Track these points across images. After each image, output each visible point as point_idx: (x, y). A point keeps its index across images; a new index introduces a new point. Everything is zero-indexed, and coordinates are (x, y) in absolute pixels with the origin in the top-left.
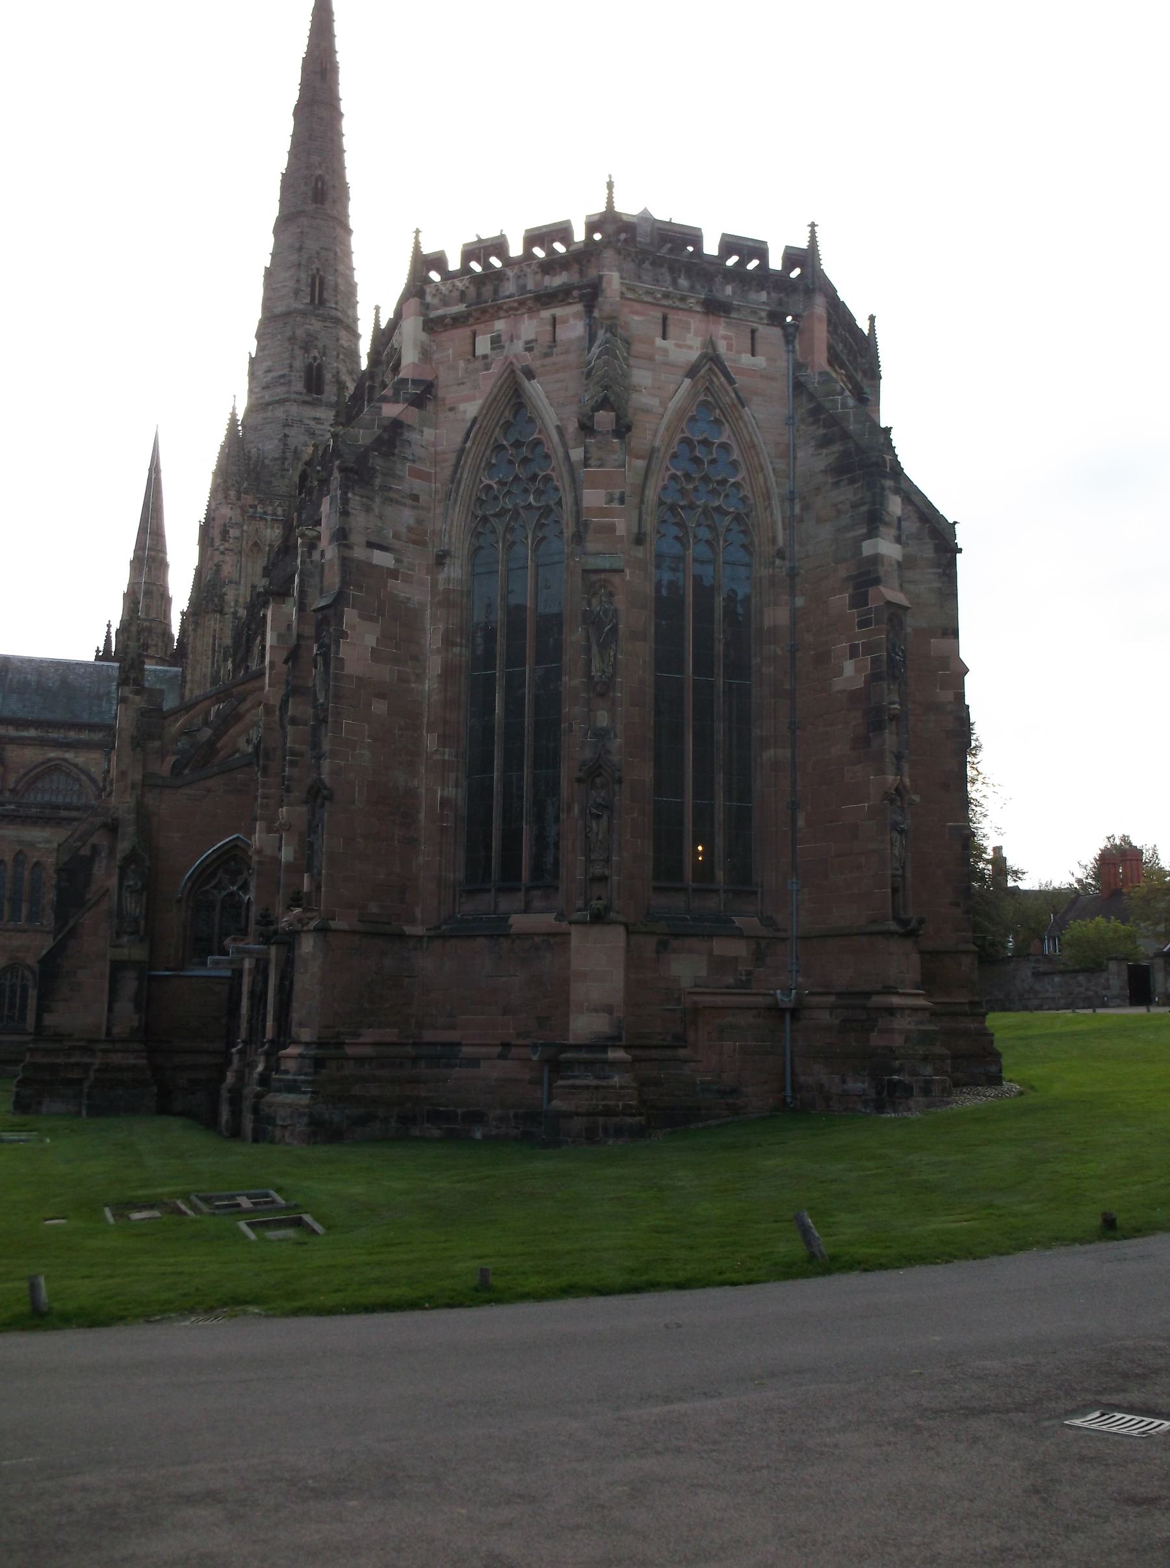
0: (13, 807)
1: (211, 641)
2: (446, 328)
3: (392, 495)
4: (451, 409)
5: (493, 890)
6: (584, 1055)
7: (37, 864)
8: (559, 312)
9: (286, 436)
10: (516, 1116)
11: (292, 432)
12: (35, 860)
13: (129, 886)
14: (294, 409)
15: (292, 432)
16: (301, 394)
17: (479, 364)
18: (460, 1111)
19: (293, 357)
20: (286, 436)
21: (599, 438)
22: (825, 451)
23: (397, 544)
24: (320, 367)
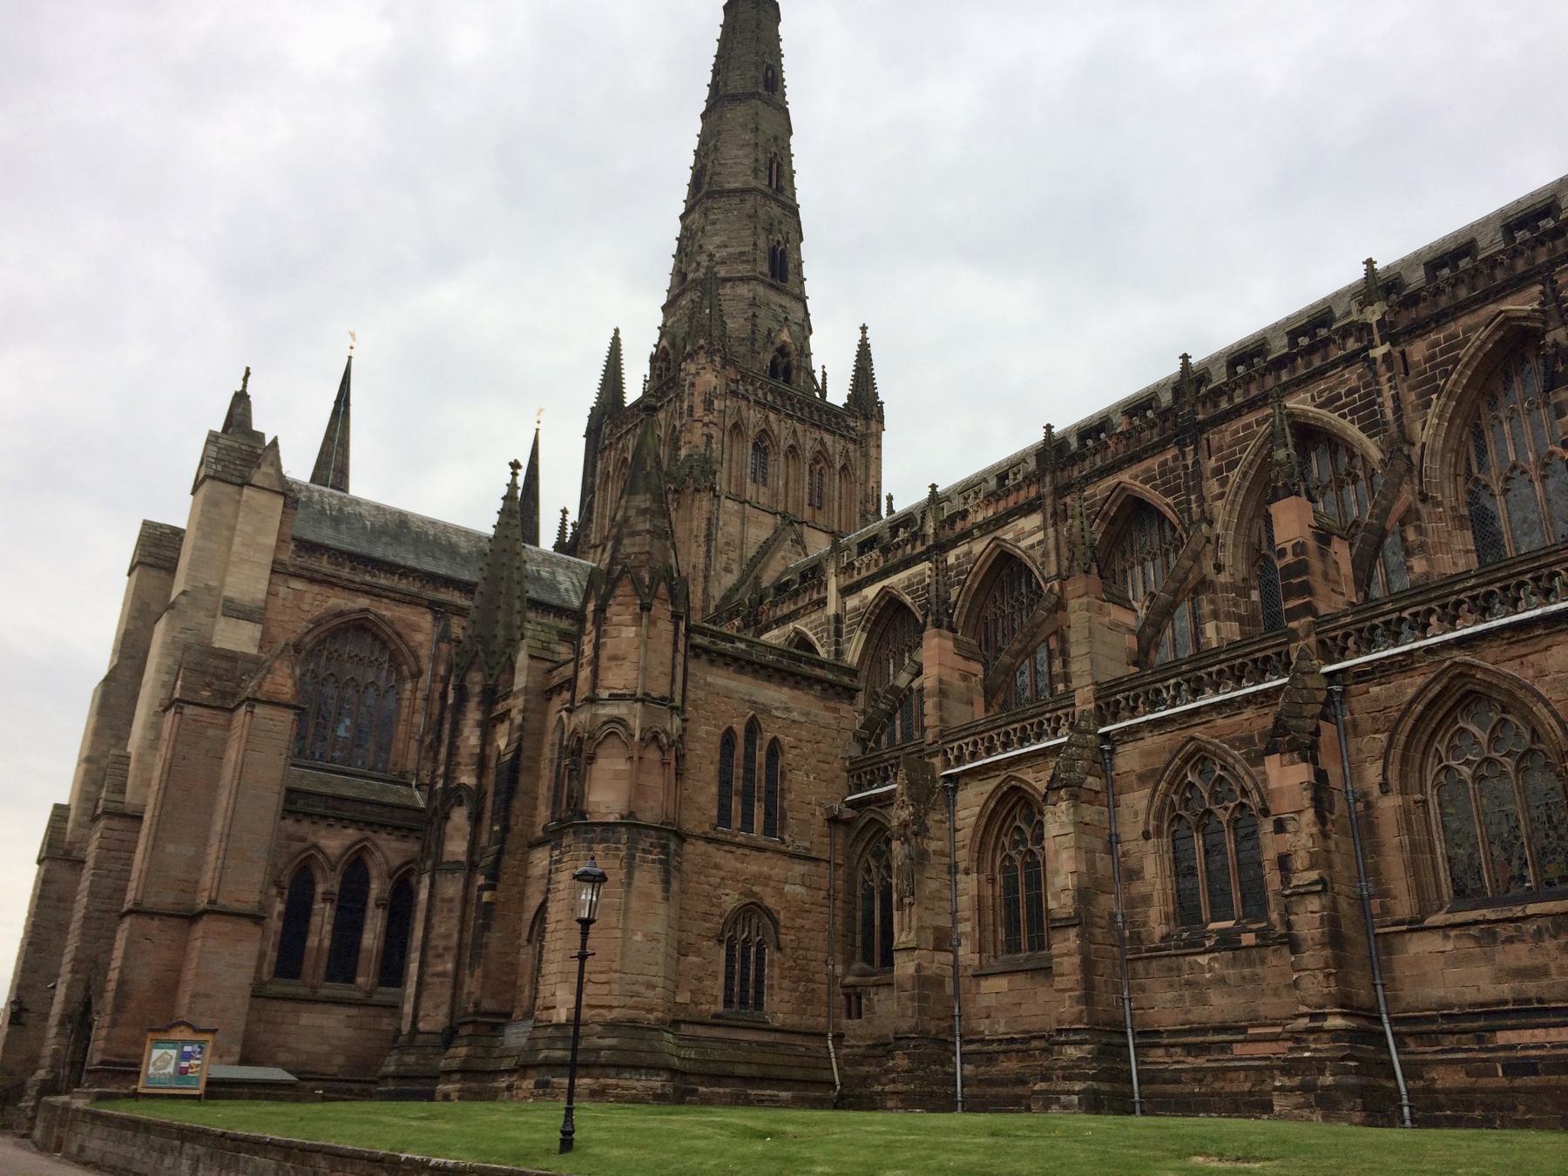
0: (743, 646)
7: (775, 740)
9: (754, 315)
12: (769, 736)
14: (761, 290)
15: (762, 313)
16: (766, 276)
19: (755, 234)
20: (754, 315)
24: (783, 252)
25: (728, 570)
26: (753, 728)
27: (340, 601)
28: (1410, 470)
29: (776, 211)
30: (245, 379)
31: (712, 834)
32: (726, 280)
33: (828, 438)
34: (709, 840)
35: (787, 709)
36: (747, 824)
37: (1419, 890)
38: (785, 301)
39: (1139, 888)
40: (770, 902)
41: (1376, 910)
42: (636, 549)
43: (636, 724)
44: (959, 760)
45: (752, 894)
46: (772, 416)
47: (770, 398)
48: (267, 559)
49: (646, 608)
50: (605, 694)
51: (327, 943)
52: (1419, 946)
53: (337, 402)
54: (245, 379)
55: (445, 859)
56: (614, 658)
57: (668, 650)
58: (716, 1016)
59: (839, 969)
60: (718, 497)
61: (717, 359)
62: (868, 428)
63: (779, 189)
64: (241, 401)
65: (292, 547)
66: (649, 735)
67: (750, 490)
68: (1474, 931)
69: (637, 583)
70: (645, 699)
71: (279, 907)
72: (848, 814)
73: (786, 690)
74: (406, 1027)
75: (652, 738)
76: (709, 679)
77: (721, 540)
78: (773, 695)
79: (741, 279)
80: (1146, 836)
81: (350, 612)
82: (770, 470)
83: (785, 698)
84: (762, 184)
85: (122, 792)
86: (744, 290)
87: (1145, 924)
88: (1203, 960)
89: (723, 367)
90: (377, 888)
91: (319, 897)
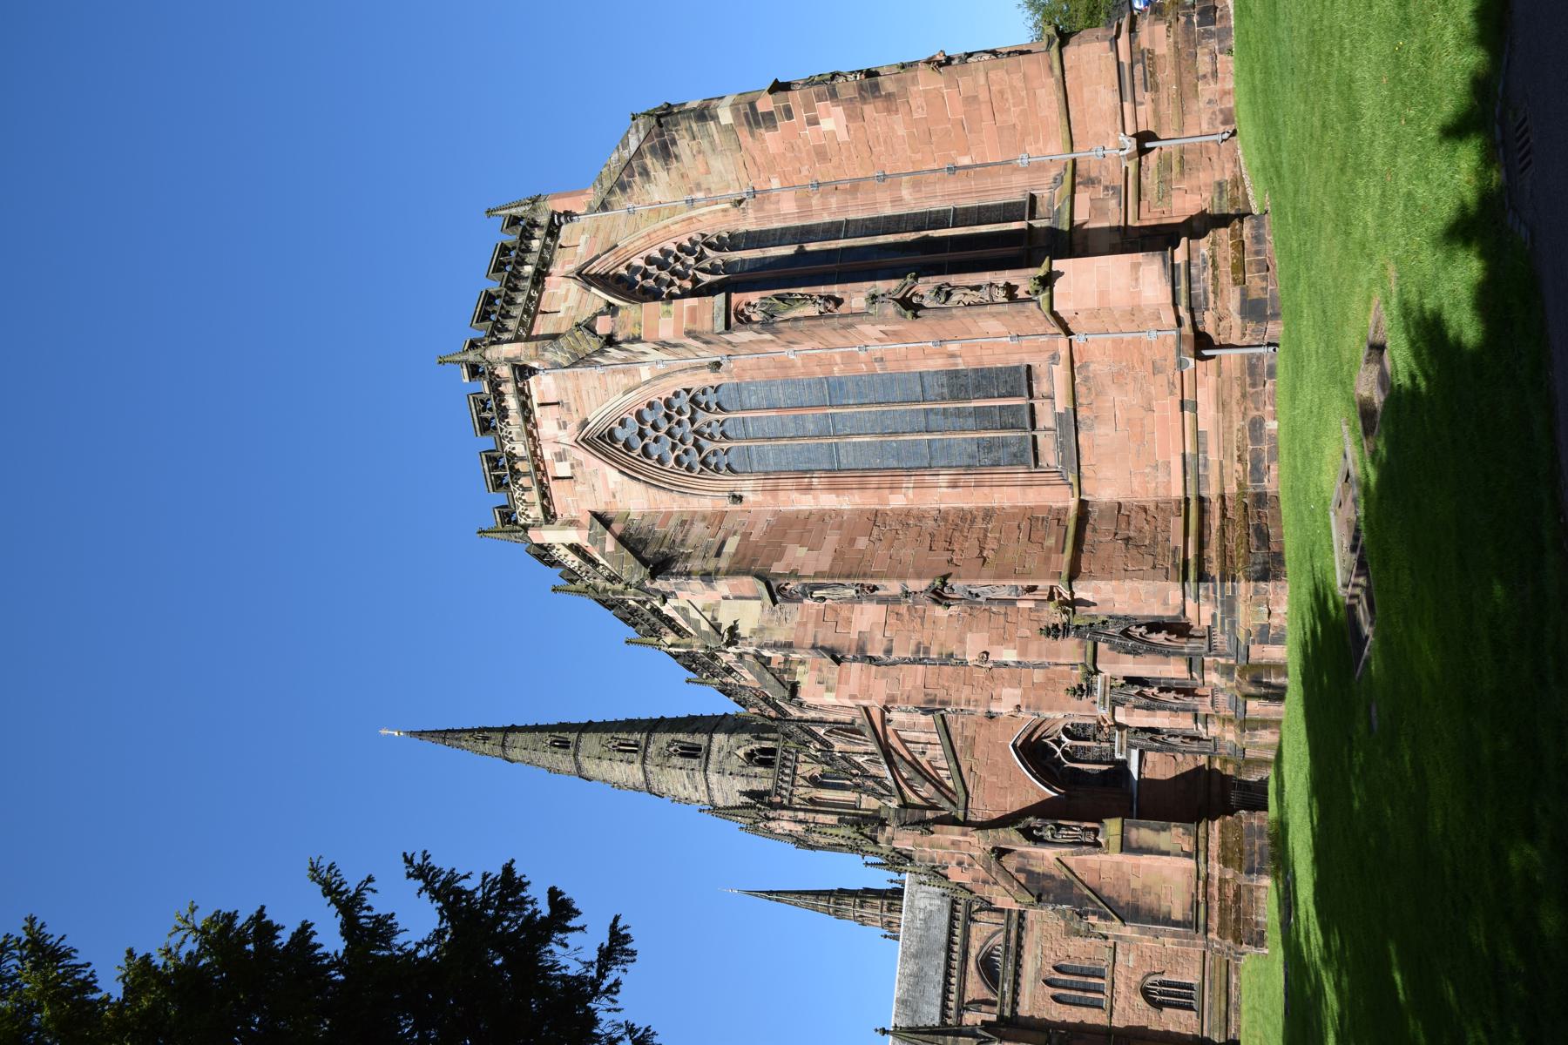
2: (550, 502)
3: (678, 541)
4: (614, 496)
5: (1034, 433)
6: (1182, 286)
7: (1055, 968)
8: (536, 400)
10: (1254, 385)
11: (728, 768)
12: (1051, 969)
13: (1053, 836)
17: (578, 471)
18: (1250, 447)
19: (675, 767)
20: (731, 774)
21: (617, 328)
22: (652, 173)
23: (721, 534)
31: (1108, 1012)
35: (1036, 957)
36: (1098, 990)
40: (1139, 978)
45: (1136, 989)
58: (1198, 1017)
84: (637, 758)
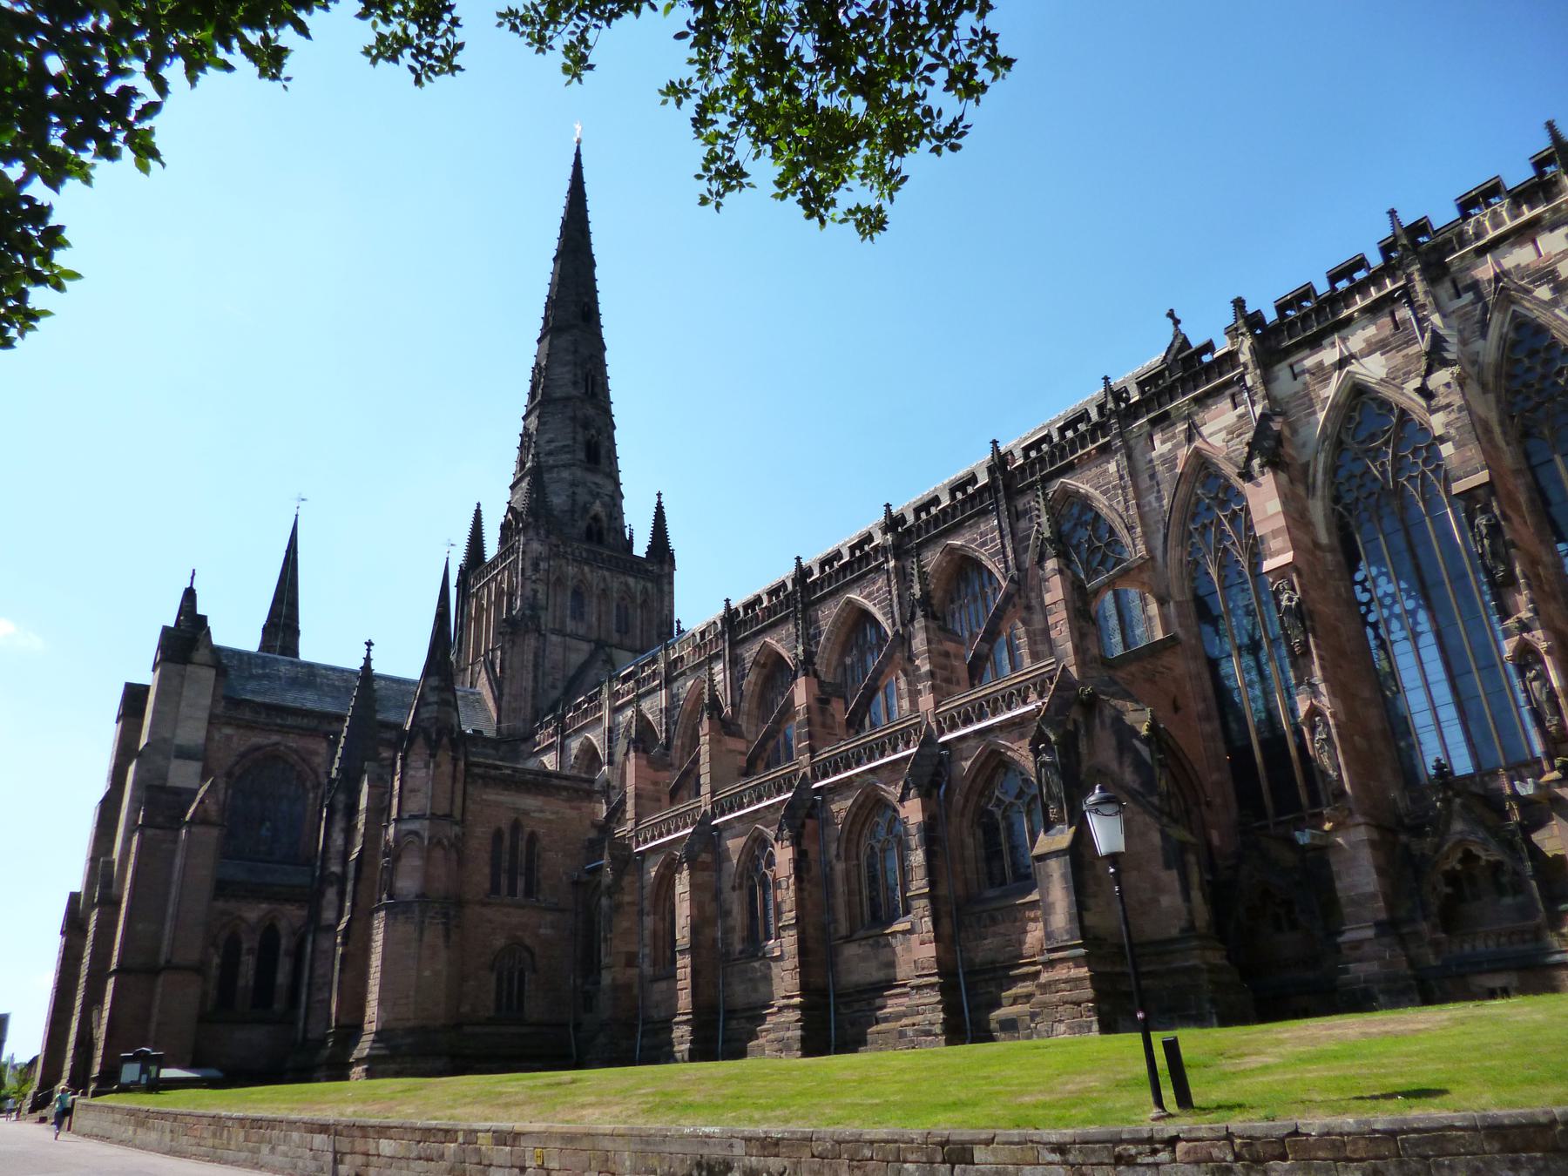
0: (508, 772)
1: (531, 657)
9: (574, 493)
11: (579, 490)
12: (528, 829)
14: (579, 473)
15: (579, 490)
19: (575, 432)
20: (574, 493)
25: (554, 687)
26: (516, 826)
27: (257, 739)
28: (903, 644)
29: (591, 411)
30: (192, 578)
32: (553, 467)
33: (631, 581)
34: (484, 904)
36: (512, 891)
37: (851, 918)
38: (599, 479)
39: (731, 922)
40: (528, 941)
41: (832, 930)
42: (427, 715)
43: (426, 835)
44: (645, 841)
46: (586, 569)
47: (584, 555)
48: (205, 715)
49: (433, 756)
50: (406, 815)
51: (251, 983)
52: (851, 950)
53: (288, 552)
54: (192, 578)
55: (324, 923)
56: (412, 791)
57: (449, 782)
59: (579, 981)
60: (544, 636)
61: (542, 532)
62: (662, 569)
63: (594, 395)
64: (190, 595)
65: (223, 703)
66: (435, 840)
67: (570, 625)
68: (871, 941)
69: (428, 739)
70: (434, 817)
71: (216, 960)
72: (585, 878)
73: (540, 798)
74: (300, 1036)
75: (435, 842)
76: (484, 797)
77: (548, 665)
78: (530, 802)
79: (564, 466)
80: (734, 888)
81: (266, 746)
82: (586, 609)
83: (540, 803)
85: (111, 887)
86: (565, 474)
87: (732, 944)
88: (757, 965)
89: (547, 537)
90: (284, 943)
91: (244, 951)
